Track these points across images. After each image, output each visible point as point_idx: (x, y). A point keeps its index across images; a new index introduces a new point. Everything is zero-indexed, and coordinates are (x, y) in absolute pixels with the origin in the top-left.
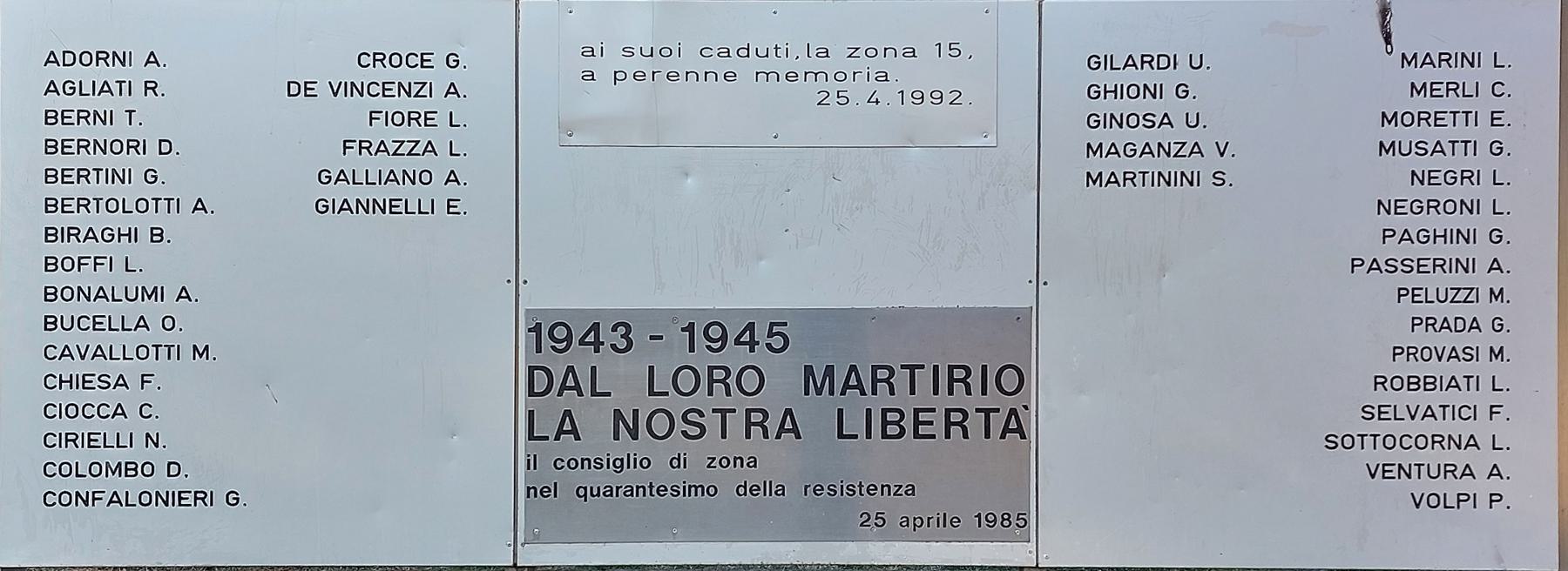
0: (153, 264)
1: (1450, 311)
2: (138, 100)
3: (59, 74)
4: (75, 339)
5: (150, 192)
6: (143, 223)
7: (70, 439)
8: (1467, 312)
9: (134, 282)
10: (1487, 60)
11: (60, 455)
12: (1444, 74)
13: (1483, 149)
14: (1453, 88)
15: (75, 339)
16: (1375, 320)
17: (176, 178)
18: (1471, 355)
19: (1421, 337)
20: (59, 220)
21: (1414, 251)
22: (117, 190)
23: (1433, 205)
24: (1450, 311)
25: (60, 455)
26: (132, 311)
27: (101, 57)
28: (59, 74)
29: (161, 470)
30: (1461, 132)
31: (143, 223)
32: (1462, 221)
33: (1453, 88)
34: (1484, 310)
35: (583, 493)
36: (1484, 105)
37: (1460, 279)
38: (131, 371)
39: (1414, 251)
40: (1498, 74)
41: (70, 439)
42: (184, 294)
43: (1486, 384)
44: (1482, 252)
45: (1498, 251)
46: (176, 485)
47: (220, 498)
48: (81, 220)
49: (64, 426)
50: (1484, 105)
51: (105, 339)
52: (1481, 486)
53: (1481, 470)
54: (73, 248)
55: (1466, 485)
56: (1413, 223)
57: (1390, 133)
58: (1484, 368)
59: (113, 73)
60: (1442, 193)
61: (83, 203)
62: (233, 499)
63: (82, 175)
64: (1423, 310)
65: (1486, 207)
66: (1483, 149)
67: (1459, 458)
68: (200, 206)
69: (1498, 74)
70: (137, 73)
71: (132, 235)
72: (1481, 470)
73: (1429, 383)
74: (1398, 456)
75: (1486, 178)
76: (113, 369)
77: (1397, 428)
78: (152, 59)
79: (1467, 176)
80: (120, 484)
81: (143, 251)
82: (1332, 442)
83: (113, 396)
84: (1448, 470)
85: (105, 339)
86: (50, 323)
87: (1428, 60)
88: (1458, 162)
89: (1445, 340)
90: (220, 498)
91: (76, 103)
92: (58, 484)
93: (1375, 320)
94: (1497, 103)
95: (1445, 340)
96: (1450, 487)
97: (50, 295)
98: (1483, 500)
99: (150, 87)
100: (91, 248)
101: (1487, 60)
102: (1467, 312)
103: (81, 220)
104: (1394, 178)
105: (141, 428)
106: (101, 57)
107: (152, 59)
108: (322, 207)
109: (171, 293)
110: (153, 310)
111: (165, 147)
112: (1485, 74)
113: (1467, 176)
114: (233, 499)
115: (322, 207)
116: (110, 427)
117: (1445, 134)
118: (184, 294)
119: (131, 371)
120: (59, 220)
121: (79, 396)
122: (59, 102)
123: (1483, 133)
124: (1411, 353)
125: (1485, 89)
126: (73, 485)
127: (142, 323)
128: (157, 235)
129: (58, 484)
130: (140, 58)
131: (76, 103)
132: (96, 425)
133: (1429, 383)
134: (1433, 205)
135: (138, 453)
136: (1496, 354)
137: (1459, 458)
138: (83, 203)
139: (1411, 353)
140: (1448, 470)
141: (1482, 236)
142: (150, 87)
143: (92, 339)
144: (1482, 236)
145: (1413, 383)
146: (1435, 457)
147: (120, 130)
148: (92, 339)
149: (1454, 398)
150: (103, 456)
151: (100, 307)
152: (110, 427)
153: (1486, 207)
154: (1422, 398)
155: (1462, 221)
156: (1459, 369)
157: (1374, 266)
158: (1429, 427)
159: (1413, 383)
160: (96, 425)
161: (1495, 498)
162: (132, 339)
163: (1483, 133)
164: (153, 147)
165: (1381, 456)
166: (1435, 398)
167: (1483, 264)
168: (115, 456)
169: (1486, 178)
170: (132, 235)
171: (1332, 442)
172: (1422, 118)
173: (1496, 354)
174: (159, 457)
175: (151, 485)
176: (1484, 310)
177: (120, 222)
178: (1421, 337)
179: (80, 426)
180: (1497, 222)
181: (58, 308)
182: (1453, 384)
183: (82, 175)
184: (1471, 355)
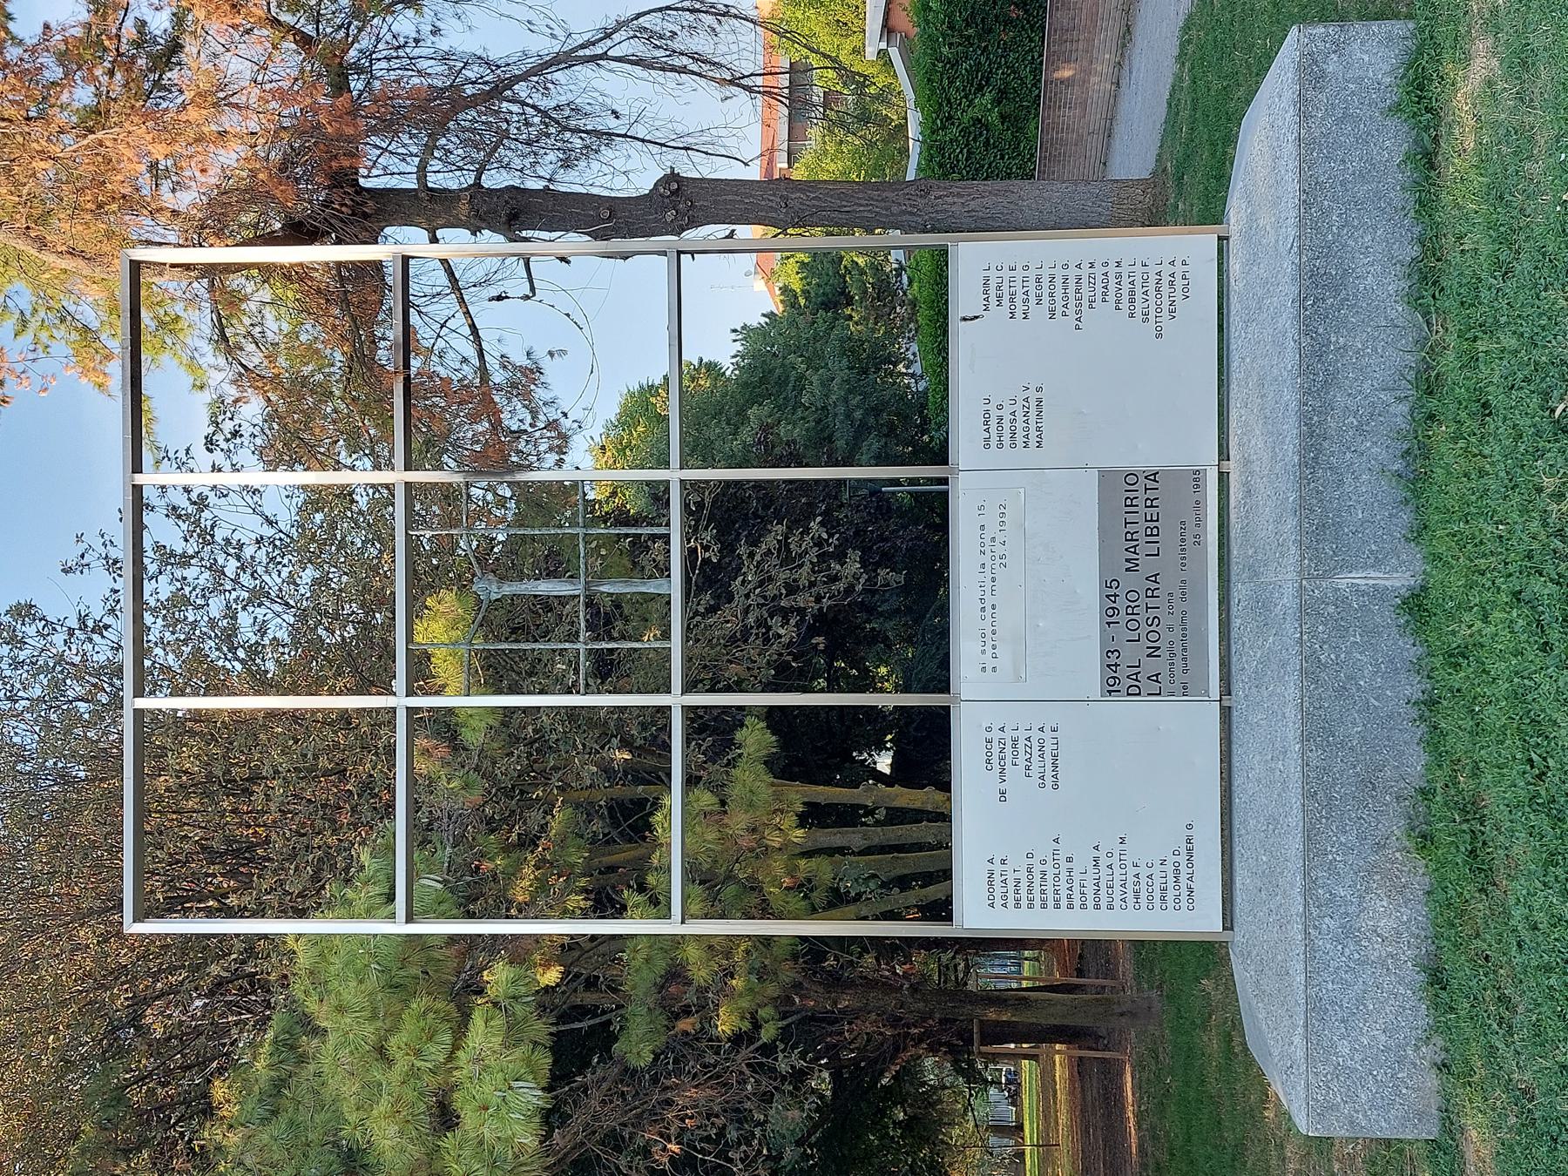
0: (1083, 862)
1: (1099, 286)
2: (1009, 867)
3: (998, 902)
4: (1117, 896)
5: (1050, 863)
6: (1064, 865)
7: (1163, 899)
8: (1099, 278)
9: (1091, 870)
10: (987, 273)
11: (1171, 904)
12: (993, 292)
13: (1026, 273)
14: (999, 288)
15: (1117, 896)
16: (1102, 317)
17: (1044, 850)
18: (1119, 276)
19: (1111, 298)
20: (1064, 902)
21: (1072, 303)
22: (1050, 877)
23: (1051, 295)
24: (1099, 286)
25: (1171, 904)
26: (1104, 871)
27: (990, 884)
28: (998, 902)
29: (1177, 858)
30: (1019, 284)
31: (1064, 865)
32: (1059, 281)
33: (999, 288)
34: (1099, 270)
35: (1185, 671)
36: (1006, 274)
37: (1085, 281)
38: (1131, 871)
39: (1072, 303)
40: (993, 268)
41: (1163, 899)
42: (1096, 848)
43: (1132, 269)
44: (1072, 273)
45: (1072, 266)
46: (1183, 851)
47: (1189, 833)
48: (1064, 893)
49: (1157, 901)
50: (1006, 274)
51: (1117, 883)
52: (1179, 269)
53: (1171, 269)
54: (1076, 896)
55: (1178, 276)
56: (1060, 303)
57: (1019, 314)
58: (1125, 270)
59: (997, 878)
60: (1046, 291)
61: (1056, 892)
62: (1190, 827)
63: (1043, 892)
64: (1099, 297)
65: (1052, 271)
66: (1026, 273)
67: (1166, 279)
68: (1056, 841)
69: (993, 268)
70: (997, 868)
71: (1070, 871)
72: (1171, 269)
73: (1132, 293)
74: (1165, 306)
75: (1039, 272)
76: (1131, 879)
77: (1153, 307)
78: (991, 861)
79: (1038, 280)
80: (1183, 878)
81: (1077, 867)
82: (1159, 336)
83: (1144, 880)
84: (1171, 283)
85: (1117, 883)
86: (1111, 908)
87: (986, 299)
88: (1032, 285)
89: (1112, 287)
90: (1189, 833)
91: (1011, 895)
92: (1184, 904)
93: (1102, 317)
94: (1006, 268)
95: (1112, 287)
96: (1179, 283)
97: (1097, 907)
98: (1185, 268)
99: (1003, 862)
100: (1076, 889)
101: (987, 273)
102: (1099, 278)
103: (1064, 893)
104: (1039, 313)
105: (1157, 868)
106: (990, 884)
107: (991, 861)
108: (1056, 786)
109: (1097, 854)
110: (1103, 862)
111: (1030, 856)
112: (993, 274)
113: (1038, 280)
114: (1190, 827)
115: (1056, 786)
116: (1158, 881)
117: (1020, 291)
118: (1096, 848)
119: (1131, 871)
120: (1064, 902)
121: (1144, 895)
122: (1011, 902)
123: (1019, 274)
124: (1118, 302)
125: (999, 274)
126: (1184, 897)
127: (1110, 867)
128: (1069, 860)
129: (1184, 904)
130: (991, 867)
131: (1011, 895)
132: (1157, 888)
133: (1132, 293)
134: (1051, 295)
135: (1170, 868)
136: (1119, 264)
137: (1166, 279)
138: (1056, 892)
139: (1118, 302)
140: (1171, 283)
141: (1065, 272)
142: (1003, 862)
143: (1117, 888)
144: (1065, 272)
145: (1132, 301)
146: (1165, 289)
147: (1023, 875)
148: (1117, 888)
149: (1138, 283)
150: (1171, 884)
151: (1103, 885)
152: (1158, 881)
153: (1052, 271)
154: (1139, 296)
155: (1059, 281)
156: (1125, 281)
157: (1079, 320)
158: (1152, 293)
159: (1132, 301)
160: (1157, 888)
161: (1184, 263)
162: (1117, 871)
163: (1019, 274)
164: (1030, 861)
165: (1165, 313)
166: (1139, 291)
167: (1079, 272)
168: (1171, 879)
169: (1039, 272)
170: (1070, 871)
171: (1159, 336)
172: (1012, 301)
173: (1119, 264)
174: (1171, 859)
175: (1184, 862)
176: (1099, 270)
177: (1064, 876)
178: (1111, 298)
179: (1157, 894)
180: (1059, 266)
181: (1104, 904)
182: (1132, 283)
183: (1043, 892)
184: (1119, 276)
